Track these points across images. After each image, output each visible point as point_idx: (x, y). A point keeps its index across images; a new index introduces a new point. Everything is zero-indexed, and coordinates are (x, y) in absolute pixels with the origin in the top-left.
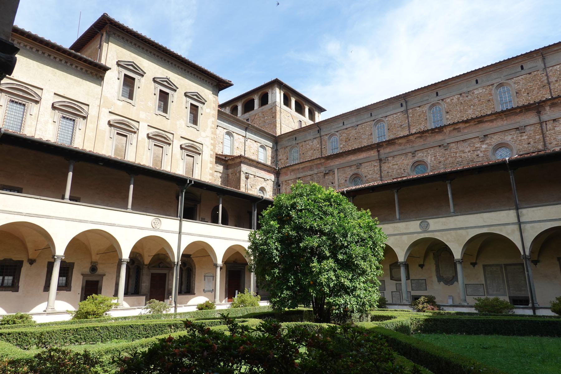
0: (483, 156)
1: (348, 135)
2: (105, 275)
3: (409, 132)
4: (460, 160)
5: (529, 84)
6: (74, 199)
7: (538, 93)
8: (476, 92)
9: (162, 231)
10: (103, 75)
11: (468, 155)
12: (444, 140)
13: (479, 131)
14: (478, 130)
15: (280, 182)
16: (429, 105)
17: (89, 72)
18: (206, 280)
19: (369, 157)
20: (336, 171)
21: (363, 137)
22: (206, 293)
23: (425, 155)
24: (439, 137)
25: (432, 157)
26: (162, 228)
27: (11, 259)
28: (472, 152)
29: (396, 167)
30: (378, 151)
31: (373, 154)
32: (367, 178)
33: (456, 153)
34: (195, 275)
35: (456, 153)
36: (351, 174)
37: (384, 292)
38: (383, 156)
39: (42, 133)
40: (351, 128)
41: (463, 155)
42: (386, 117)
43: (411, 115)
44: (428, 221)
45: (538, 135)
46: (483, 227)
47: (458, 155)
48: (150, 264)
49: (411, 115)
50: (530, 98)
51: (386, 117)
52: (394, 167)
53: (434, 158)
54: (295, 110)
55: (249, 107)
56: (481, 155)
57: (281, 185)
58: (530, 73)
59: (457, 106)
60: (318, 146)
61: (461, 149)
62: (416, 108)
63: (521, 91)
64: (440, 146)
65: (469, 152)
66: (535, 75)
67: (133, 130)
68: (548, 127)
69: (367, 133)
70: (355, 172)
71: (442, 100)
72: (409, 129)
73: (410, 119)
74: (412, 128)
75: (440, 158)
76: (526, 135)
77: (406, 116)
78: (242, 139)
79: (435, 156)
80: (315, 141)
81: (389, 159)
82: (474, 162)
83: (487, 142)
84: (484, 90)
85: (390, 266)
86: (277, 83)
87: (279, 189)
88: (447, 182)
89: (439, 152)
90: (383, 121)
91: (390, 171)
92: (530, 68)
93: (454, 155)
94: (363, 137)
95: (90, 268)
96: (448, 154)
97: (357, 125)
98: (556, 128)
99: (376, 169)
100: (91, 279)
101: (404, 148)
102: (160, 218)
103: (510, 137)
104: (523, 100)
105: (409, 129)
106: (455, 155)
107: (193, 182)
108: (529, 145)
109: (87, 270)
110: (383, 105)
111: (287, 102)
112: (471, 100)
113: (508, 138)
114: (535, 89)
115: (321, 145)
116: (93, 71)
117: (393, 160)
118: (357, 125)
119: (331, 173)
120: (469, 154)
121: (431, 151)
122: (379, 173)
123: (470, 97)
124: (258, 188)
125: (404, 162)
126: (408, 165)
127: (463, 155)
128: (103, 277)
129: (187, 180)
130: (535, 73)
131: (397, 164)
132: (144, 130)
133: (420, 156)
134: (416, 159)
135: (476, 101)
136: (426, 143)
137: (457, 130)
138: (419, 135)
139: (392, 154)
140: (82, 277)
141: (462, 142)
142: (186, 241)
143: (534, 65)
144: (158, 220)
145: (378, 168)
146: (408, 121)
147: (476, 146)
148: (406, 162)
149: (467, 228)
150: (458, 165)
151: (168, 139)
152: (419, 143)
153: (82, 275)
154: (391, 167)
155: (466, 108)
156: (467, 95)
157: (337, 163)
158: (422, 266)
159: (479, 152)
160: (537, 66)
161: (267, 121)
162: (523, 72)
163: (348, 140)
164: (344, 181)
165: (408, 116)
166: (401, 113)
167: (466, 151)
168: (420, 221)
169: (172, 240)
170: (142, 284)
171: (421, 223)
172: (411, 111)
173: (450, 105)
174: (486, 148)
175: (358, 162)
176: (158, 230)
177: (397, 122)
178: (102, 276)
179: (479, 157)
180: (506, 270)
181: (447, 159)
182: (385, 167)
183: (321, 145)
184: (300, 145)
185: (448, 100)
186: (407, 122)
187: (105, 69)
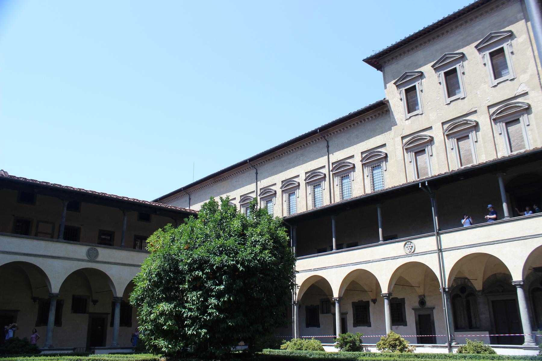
2: (434, 308)
6: (340, 247)
9: (418, 254)
10: (415, 98)
17: (377, 115)
39: (361, 190)
67: (426, 140)
95: (419, 302)
100: (422, 312)
109: (417, 305)
116: (379, 112)
128: (433, 311)
129: (418, 185)
132: (438, 134)
140: (413, 312)
144: (410, 243)
153: (413, 309)
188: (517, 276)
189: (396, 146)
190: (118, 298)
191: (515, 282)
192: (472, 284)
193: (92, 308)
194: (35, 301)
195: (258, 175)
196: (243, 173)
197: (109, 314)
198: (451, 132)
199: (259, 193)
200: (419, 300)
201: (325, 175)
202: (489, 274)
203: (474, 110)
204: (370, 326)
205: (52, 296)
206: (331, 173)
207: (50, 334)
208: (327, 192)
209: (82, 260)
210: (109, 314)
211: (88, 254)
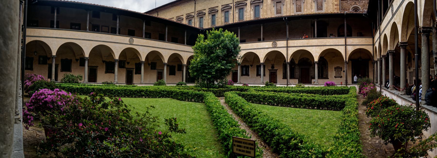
2: (277, 70)
9: (278, 48)
18: (336, 70)
22: (337, 78)
26: (278, 46)
27: (246, 65)
34: (328, 68)
100: (272, 71)
102: (276, 42)
140: (269, 71)
142: (292, 51)
153: (269, 70)
169: (283, 51)
176: (275, 47)
188: (316, 59)
190: (143, 61)
191: (315, 62)
192: (294, 61)
193: (127, 66)
194: (104, 63)
195: (196, 4)
196: (188, 3)
197: (134, 68)
199: (196, 13)
201: (231, 7)
202: (301, 58)
204: (249, 76)
205: (116, 61)
206: (234, 6)
207: (116, 77)
208: (232, 15)
209: (127, 44)
210: (134, 68)
211: (130, 41)
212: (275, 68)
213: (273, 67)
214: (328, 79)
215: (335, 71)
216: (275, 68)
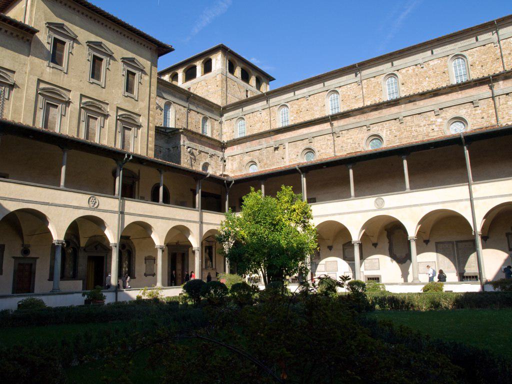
0: (438, 131)
1: (300, 106)
2: (37, 258)
3: (364, 104)
4: (415, 134)
5: (483, 56)
7: (491, 66)
8: (431, 63)
11: (424, 130)
12: (400, 113)
13: (435, 105)
14: (433, 103)
15: (226, 157)
16: (385, 75)
17: (15, 34)
18: (147, 263)
19: (322, 130)
20: (287, 145)
21: (316, 108)
23: (380, 128)
24: (394, 110)
25: (387, 131)
28: (427, 126)
29: (350, 141)
30: (332, 125)
31: (326, 126)
32: (320, 153)
33: (411, 127)
34: (135, 258)
35: (411, 127)
36: (303, 148)
37: (336, 273)
38: (337, 130)
40: (302, 99)
41: (418, 129)
42: (340, 87)
43: (366, 86)
44: (383, 197)
45: (491, 109)
46: (438, 203)
47: (413, 129)
48: (86, 247)
49: (366, 86)
50: (483, 71)
51: (340, 87)
52: (349, 141)
53: (389, 132)
54: (241, 78)
55: (190, 74)
56: (436, 129)
57: (227, 161)
58: (484, 45)
59: (412, 77)
60: (267, 118)
61: (416, 122)
62: (371, 79)
63: (475, 63)
64: (395, 119)
65: (424, 126)
66: (489, 48)
67: (64, 100)
68: (501, 102)
69: (319, 104)
70: (308, 146)
71: (398, 70)
72: (363, 101)
73: (364, 90)
74: (366, 99)
75: (396, 131)
76: (480, 110)
77: (360, 86)
78: (184, 110)
79: (390, 130)
80: (264, 113)
81: (343, 132)
82: (429, 137)
83: (442, 115)
84: (439, 62)
85: (344, 245)
86: (222, 48)
87: (225, 165)
88: (403, 157)
89: (394, 125)
90: (337, 92)
91: (344, 145)
92: (484, 40)
93: (409, 128)
94: (316, 108)
95: (22, 251)
96: (403, 127)
97: (309, 96)
98: (508, 103)
99: (329, 143)
100: (22, 262)
101: (359, 120)
103: (464, 111)
104: (477, 73)
105: (363, 101)
106: (410, 129)
107: (131, 156)
108: (483, 119)
109: (19, 254)
110: (337, 74)
111: (232, 70)
112: (426, 72)
113: (462, 112)
114: (489, 62)
115: (270, 117)
117: (347, 133)
118: (309, 96)
119: (281, 147)
120: (425, 128)
121: (386, 124)
122: (333, 148)
123: (425, 68)
124: (202, 164)
125: (358, 136)
126: (362, 139)
127: (418, 129)
128: (36, 261)
130: (489, 45)
131: (351, 138)
133: (375, 130)
134: (371, 133)
135: (431, 72)
136: (381, 116)
137: (413, 103)
138: (375, 107)
139: (346, 128)
140: (13, 260)
141: (417, 115)
143: (489, 37)
145: (332, 142)
146: (363, 92)
147: (432, 120)
148: (360, 136)
149: (422, 205)
150: (413, 139)
151: (102, 109)
152: (374, 115)
153: (14, 257)
154: (345, 141)
155: (421, 79)
156: (422, 66)
157: (288, 137)
158: (375, 245)
159: (434, 126)
160: (491, 38)
161: (211, 91)
162: (477, 44)
163: (299, 112)
164: (295, 156)
165: (362, 87)
166: (356, 84)
167: (422, 125)
168: (375, 198)
170: (79, 268)
171: (376, 200)
172: (365, 81)
173: (405, 76)
174: (441, 122)
175: (310, 135)
176: (96, 209)
177: (352, 93)
178: (35, 259)
179: (434, 132)
180: (457, 246)
181: (402, 133)
182: (338, 141)
183: (270, 117)
184: (248, 116)
185: (404, 71)
186: (361, 93)
187: (32, 32)
189: (30, 83)
198: (87, 107)
200: (22, 248)
203: (107, 102)
212: (32, 255)
213: (26, 251)
214: (135, 278)
215: (145, 263)
216: (32, 255)
